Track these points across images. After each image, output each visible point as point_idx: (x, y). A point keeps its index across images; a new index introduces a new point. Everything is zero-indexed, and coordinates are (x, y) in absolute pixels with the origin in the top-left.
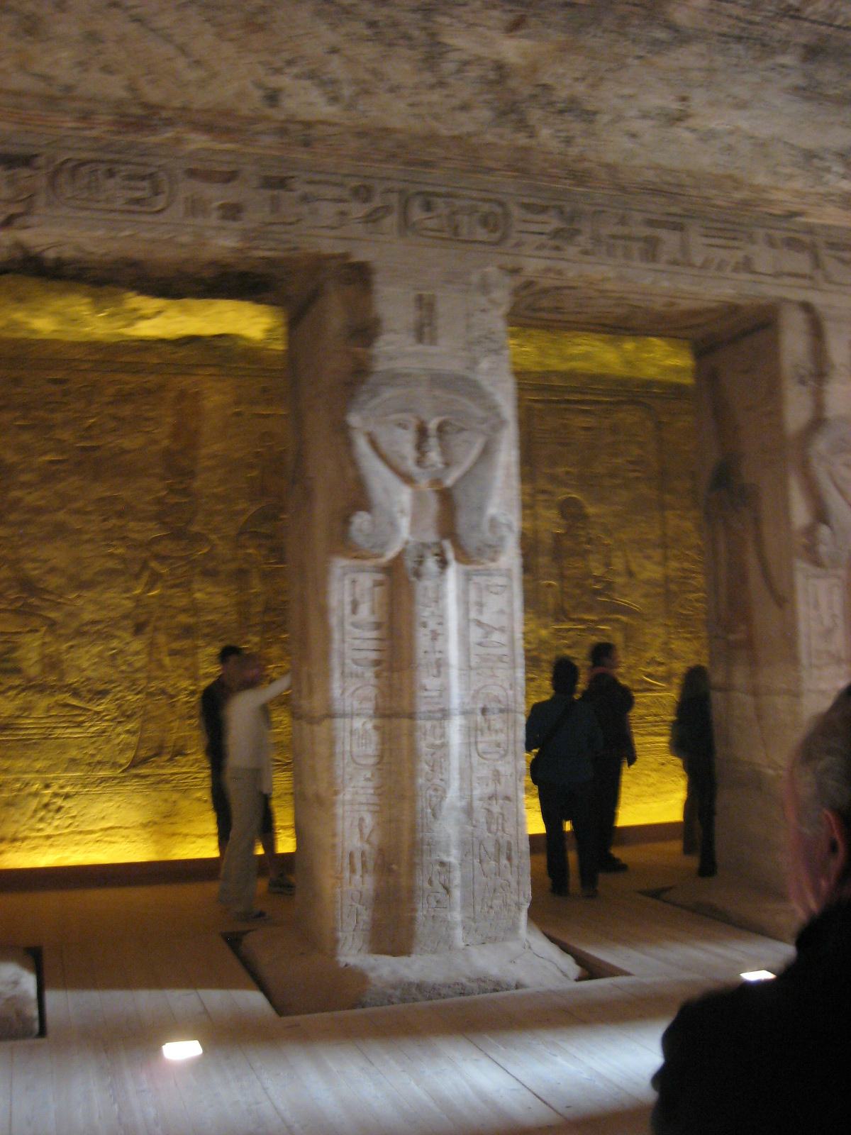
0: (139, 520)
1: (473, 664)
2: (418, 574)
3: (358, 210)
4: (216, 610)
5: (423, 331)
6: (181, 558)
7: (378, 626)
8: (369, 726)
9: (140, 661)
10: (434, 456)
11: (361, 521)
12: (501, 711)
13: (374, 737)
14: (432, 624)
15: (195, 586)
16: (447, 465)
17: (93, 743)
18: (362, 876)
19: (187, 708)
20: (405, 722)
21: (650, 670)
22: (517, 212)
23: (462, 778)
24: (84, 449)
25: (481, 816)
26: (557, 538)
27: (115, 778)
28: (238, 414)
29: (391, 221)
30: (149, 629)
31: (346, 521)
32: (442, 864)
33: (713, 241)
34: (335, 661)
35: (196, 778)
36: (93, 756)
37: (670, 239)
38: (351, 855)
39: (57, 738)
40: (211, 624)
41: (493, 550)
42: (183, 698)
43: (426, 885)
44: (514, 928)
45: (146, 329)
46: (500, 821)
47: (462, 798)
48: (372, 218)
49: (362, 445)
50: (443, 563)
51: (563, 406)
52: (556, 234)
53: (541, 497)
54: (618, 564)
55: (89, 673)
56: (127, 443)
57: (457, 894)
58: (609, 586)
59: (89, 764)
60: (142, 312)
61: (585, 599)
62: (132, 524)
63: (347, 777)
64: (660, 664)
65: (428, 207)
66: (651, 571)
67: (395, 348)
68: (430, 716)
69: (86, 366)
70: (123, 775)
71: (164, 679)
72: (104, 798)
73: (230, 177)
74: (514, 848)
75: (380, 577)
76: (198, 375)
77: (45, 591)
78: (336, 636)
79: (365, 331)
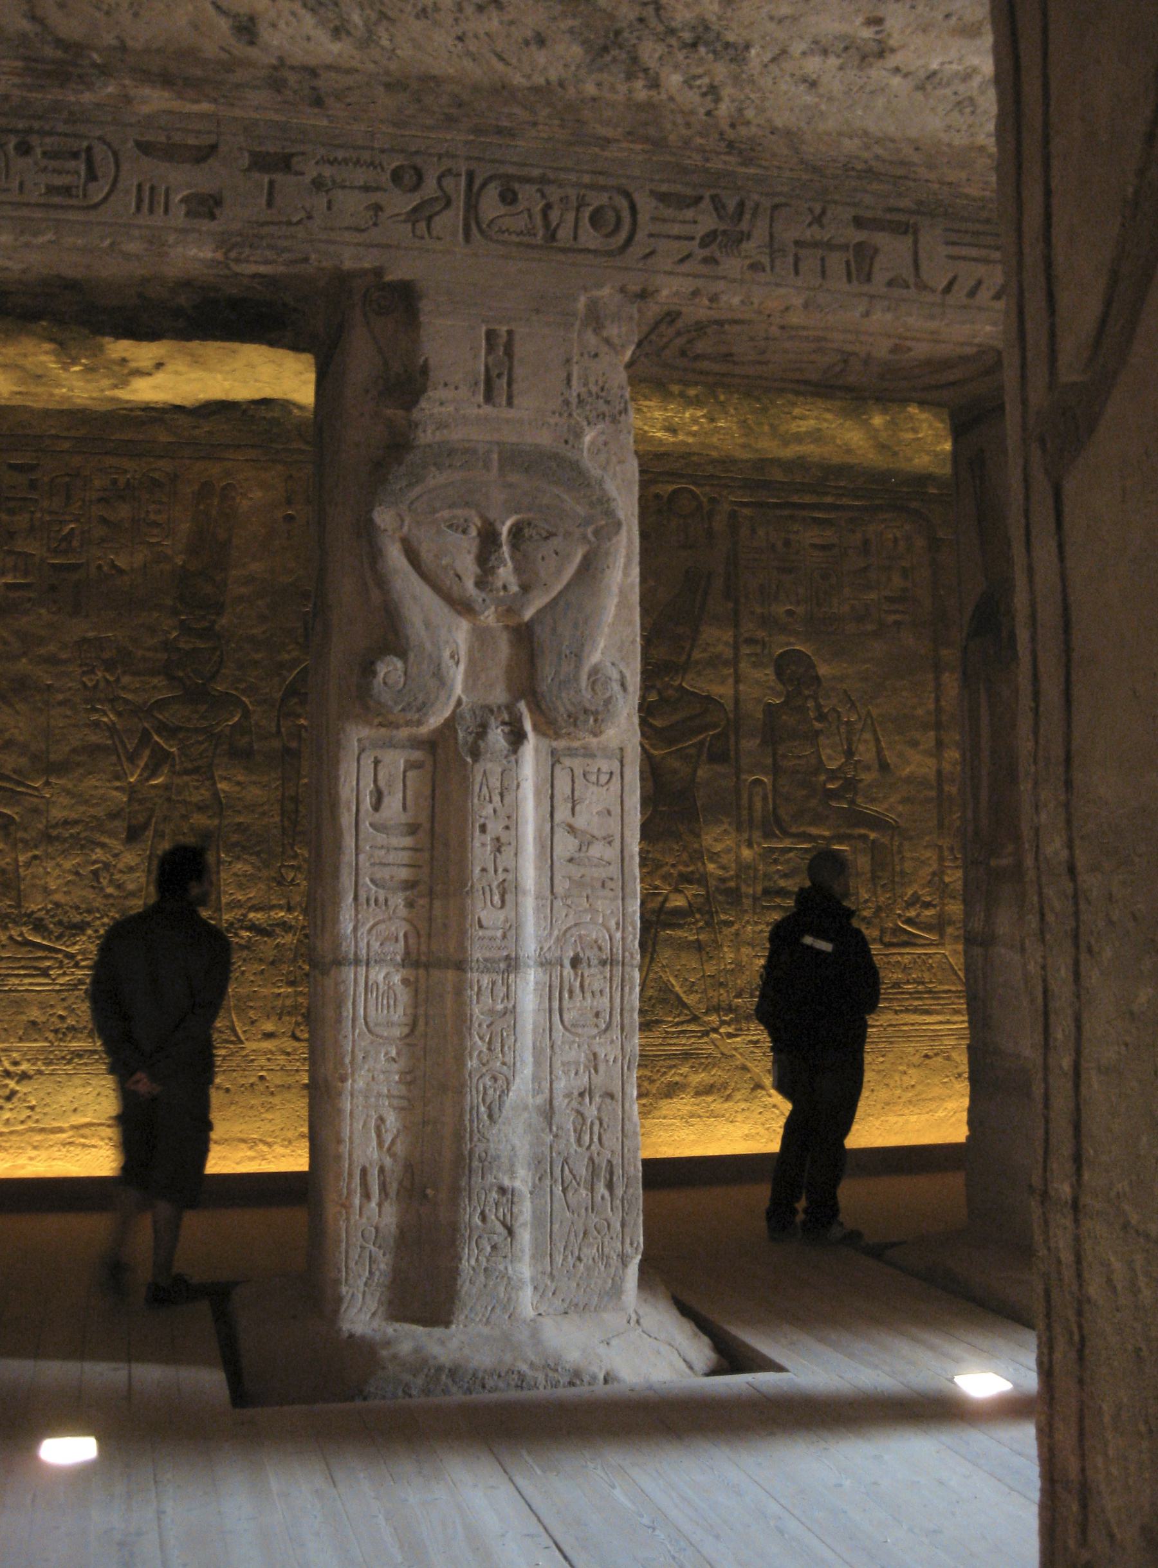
1: (559, 889)
2: (476, 754)
3: (400, 202)
5: (495, 385)
6: (196, 730)
7: (413, 829)
8: (397, 979)
10: (506, 573)
11: (389, 669)
12: (603, 963)
13: (403, 996)
14: (495, 828)
15: (218, 773)
16: (525, 588)
17: (63, 1000)
18: (380, 1205)
20: (451, 975)
21: (912, 913)
22: (646, 205)
23: (537, 1063)
25: (566, 1120)
26: (769, 709)
28: (289, 519)
29: (451, 220)
30: (150, 833)
31: (368, 670)
32: (502, 1190)
33: (964, 251)
34: (347, 881)
36: (61, 1018)
37: (893, 250)
38: (364, 1172)
39: (10, 991)
40: (240, 828)
41: (595, 716)
43: (477, 1220)
44: (616, 1291)
45: (147, 391)
46: (596, 1128)
47: (537, 1092)
48: (422, 215)
49: (395, 555)
50: (517, 738)
51: (786, 512)
52: (709, 239)
53: (746, 650)
54: (865, 752)
55: (58, 897)
56: (121, 563)
57: (525, 1236)
58: (851, 785)
59: (56, 1031)
60: (133, 365)
61: (813, 803)
62: (126, 680)
63: (360, 1055)
64: (927, 905)
65: (508, 197)
66: (917, 763)
67: (451, 409)
68: (489, 965)
69: (66, 445)
72: (77, 1081)
73: (204, 154)
74: (618, 1171)
75: (417, 755)
76: (229, 459)
78: (349, 841)
79: (407, 384)
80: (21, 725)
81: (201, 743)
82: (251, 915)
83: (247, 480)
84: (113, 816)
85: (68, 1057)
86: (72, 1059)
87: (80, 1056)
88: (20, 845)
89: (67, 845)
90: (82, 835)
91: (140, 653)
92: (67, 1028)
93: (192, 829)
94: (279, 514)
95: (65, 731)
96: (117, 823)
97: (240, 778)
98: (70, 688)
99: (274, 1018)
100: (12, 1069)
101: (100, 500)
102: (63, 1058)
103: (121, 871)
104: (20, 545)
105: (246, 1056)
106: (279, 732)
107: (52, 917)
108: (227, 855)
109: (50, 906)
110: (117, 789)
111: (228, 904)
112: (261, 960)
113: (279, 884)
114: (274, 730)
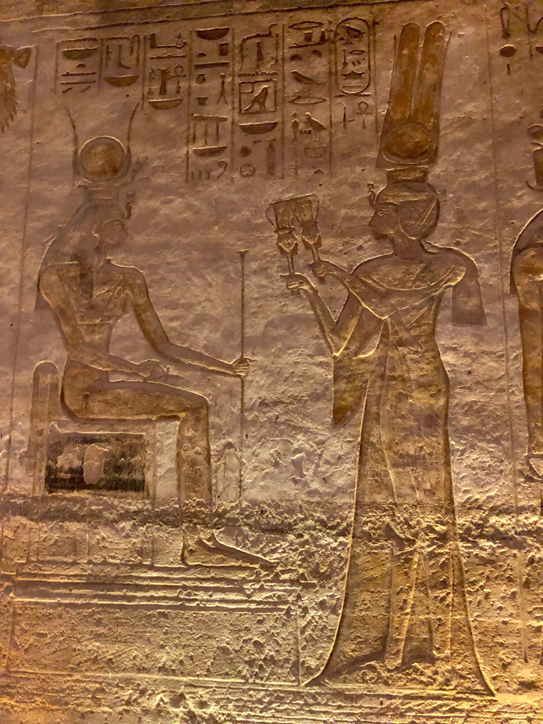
0: (342, 235)
4: (484, 384)
9: (345, 475)
15: (442, 342)
17: (260, 622)
19: (431, 567)
24: (249, 130)
27: (298, 695)
28: (507, 52)
35: (453, 710)
39: (198, 608)
40: (470, 409)
42: (423, 545)
70: (315, 689)
71: (391, 510)
77: (189, 353)
80: (213, 297)
81: (421, 307)
82: (493, 520)
83: (454, 17)
84: (316, 397)
85: (266, 700)
86: (270, 703)
87: (280, 699)
88: (212, 432)
89: (265, 430)
90: (282, 419)
91: (343, 211)
92: (265, 660)
93: (411, 412)
94: (496, 49)
95: (261, 303)
96: (321, 405)
97: (470, 348)
98: (266, 255)
99: (534, 662)
100: (198, 711)
101: (294, 58)
102: (260, 701)
103: (327, 462)
104: (210, 110)
105: (498, 713)
106: (514, 290)
107: (247, 517)
108: (458, 442)
109: (245, 504)
110: (320, 364)
111: (463, 505)
112: (510, 579)
113: (529, 479)
114: (507, 288)
